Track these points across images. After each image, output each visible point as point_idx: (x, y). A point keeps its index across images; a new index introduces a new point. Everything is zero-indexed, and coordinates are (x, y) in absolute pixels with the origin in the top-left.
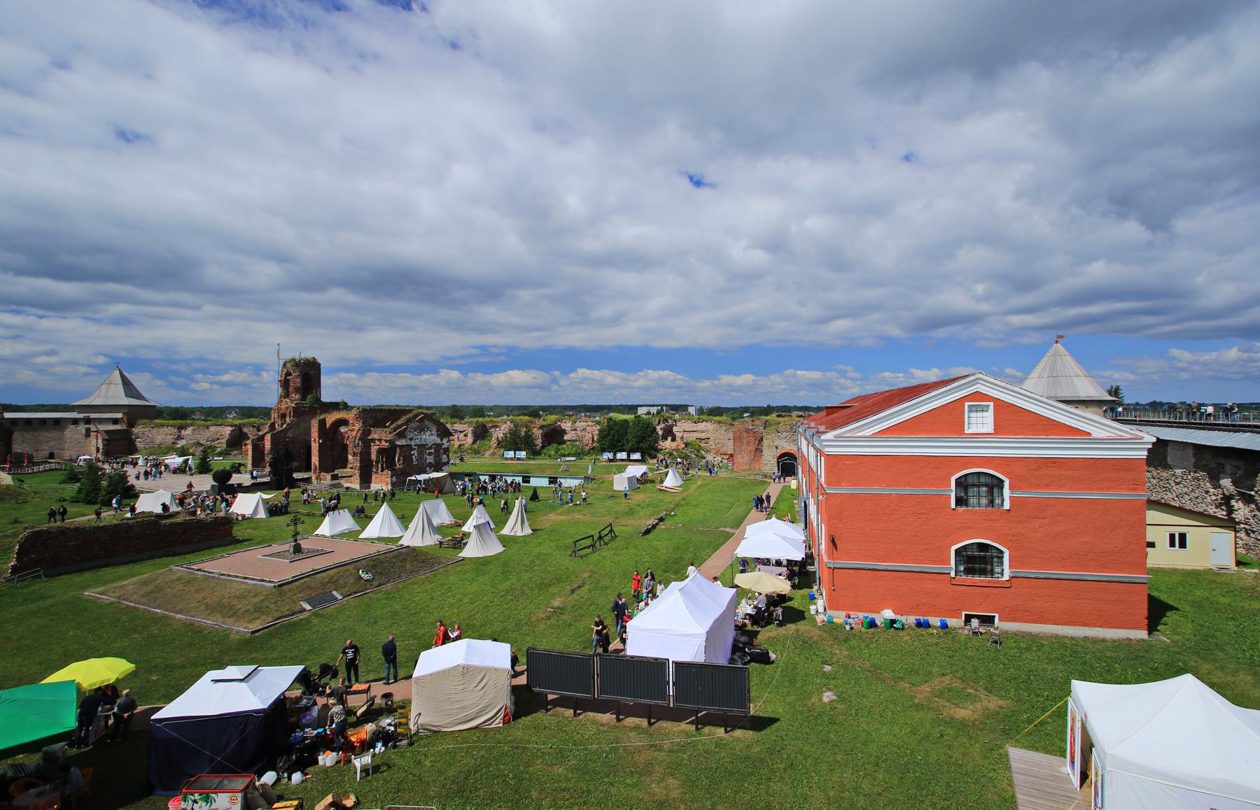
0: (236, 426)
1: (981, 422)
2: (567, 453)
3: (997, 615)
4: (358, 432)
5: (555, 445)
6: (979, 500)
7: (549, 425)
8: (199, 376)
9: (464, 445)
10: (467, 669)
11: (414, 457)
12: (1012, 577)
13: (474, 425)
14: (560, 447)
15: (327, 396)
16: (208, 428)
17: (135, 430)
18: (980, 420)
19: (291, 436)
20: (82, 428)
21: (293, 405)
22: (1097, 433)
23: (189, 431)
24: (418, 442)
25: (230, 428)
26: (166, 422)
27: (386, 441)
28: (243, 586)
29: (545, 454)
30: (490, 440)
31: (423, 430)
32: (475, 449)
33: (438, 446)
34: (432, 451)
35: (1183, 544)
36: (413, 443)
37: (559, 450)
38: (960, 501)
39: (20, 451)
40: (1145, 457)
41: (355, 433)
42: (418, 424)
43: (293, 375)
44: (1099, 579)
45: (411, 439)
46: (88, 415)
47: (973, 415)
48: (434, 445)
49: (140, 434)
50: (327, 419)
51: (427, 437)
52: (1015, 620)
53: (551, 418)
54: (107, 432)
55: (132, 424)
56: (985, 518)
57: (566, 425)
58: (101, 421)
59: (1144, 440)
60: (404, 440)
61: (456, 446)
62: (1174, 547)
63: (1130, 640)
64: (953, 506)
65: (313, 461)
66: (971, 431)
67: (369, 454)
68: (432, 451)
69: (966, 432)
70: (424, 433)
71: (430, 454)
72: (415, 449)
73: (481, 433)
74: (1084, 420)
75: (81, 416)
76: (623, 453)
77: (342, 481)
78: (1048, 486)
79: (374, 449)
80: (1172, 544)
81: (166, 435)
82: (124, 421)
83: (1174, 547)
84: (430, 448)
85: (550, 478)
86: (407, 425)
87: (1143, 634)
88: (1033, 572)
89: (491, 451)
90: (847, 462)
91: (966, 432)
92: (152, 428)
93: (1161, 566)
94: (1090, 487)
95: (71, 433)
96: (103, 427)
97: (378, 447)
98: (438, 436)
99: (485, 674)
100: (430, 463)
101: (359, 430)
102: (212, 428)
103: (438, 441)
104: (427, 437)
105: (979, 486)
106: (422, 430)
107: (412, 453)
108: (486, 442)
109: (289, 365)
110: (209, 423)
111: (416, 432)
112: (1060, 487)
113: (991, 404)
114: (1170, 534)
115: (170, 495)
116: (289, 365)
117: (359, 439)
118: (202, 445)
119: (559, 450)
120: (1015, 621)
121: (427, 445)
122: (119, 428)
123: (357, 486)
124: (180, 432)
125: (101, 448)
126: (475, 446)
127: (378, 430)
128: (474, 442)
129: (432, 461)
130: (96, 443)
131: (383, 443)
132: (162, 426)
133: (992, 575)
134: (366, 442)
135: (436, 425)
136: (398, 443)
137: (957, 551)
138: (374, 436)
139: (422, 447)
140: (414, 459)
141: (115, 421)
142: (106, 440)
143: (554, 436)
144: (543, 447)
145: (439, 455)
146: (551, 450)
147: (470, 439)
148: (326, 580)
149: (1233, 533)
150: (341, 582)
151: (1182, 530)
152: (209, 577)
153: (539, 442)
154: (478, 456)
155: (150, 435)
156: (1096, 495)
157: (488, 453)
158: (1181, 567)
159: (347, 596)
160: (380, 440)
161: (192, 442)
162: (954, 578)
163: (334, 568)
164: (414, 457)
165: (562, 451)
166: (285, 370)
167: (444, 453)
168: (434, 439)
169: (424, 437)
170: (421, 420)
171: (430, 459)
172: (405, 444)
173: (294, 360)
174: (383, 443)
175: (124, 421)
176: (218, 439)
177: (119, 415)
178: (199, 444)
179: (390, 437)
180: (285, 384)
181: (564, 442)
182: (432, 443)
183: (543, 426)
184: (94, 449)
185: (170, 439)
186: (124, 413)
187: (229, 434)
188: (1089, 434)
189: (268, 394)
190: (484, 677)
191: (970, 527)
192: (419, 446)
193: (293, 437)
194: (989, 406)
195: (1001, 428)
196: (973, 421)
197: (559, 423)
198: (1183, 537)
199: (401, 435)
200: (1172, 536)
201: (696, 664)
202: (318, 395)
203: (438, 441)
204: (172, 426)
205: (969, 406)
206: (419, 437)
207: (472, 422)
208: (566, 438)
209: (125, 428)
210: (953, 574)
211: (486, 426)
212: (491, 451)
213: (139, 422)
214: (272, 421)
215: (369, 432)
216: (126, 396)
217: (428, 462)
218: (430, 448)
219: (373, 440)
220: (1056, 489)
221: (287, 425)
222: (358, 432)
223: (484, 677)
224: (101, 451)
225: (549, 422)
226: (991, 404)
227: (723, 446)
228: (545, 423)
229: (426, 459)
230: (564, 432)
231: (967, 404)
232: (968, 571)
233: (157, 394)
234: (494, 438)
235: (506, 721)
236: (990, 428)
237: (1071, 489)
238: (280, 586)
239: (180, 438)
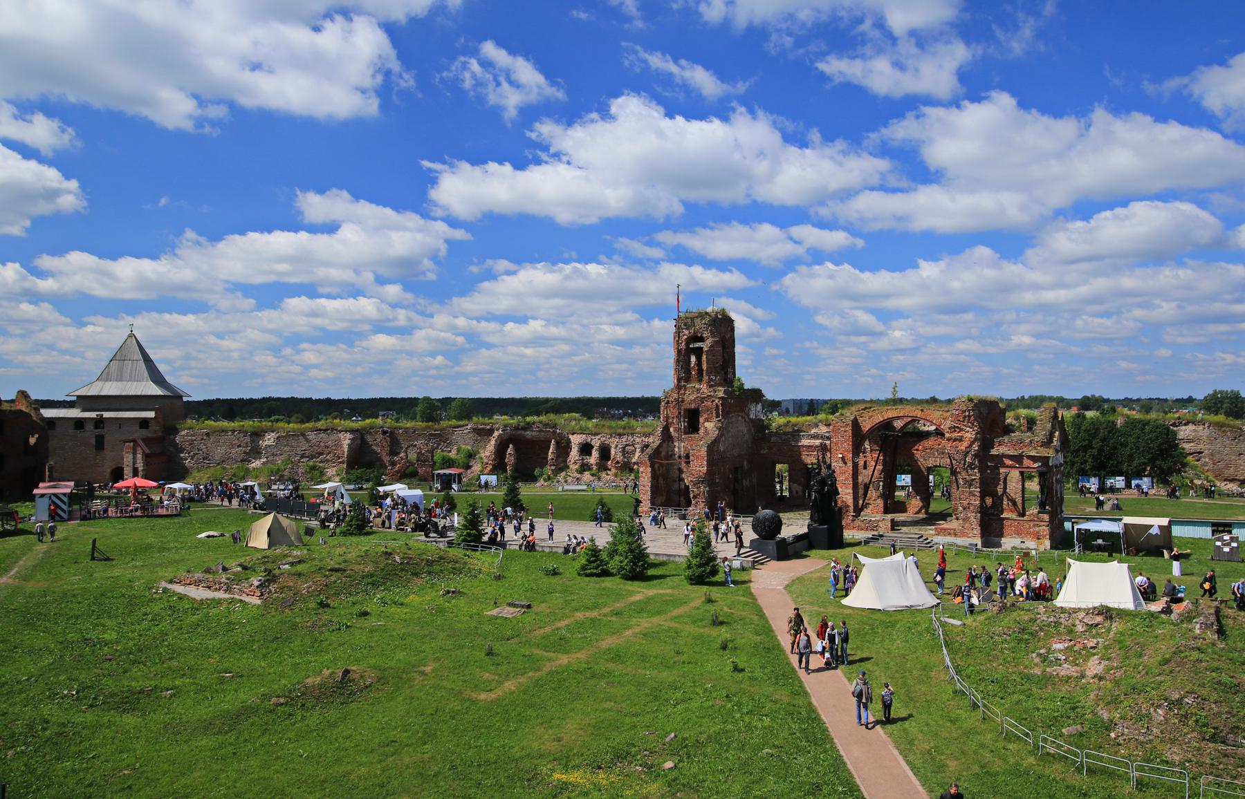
0: (357, 430)
4: (972, 443)
8: (305, 346)
21: (721, 394)
25: (349, 436)
27: (1033, 459)
41: (966, 444)
50: (860, 420)
75: (93, 415)
76: (1117, 478)
81: (232, 446)
85: (1214, 525)
101: (976, 439)
117: (976, 456)
125: (141, 469)
141: (144, 423)
155: (202, 446)
160: (1018, 459)
166: (686, 332)
173: (707, 313)
176: (321, 454)
177: (151, 414)
187: (349, 445)
193: (724, 451)
219: (1001, 457)
227: (1227, 467)
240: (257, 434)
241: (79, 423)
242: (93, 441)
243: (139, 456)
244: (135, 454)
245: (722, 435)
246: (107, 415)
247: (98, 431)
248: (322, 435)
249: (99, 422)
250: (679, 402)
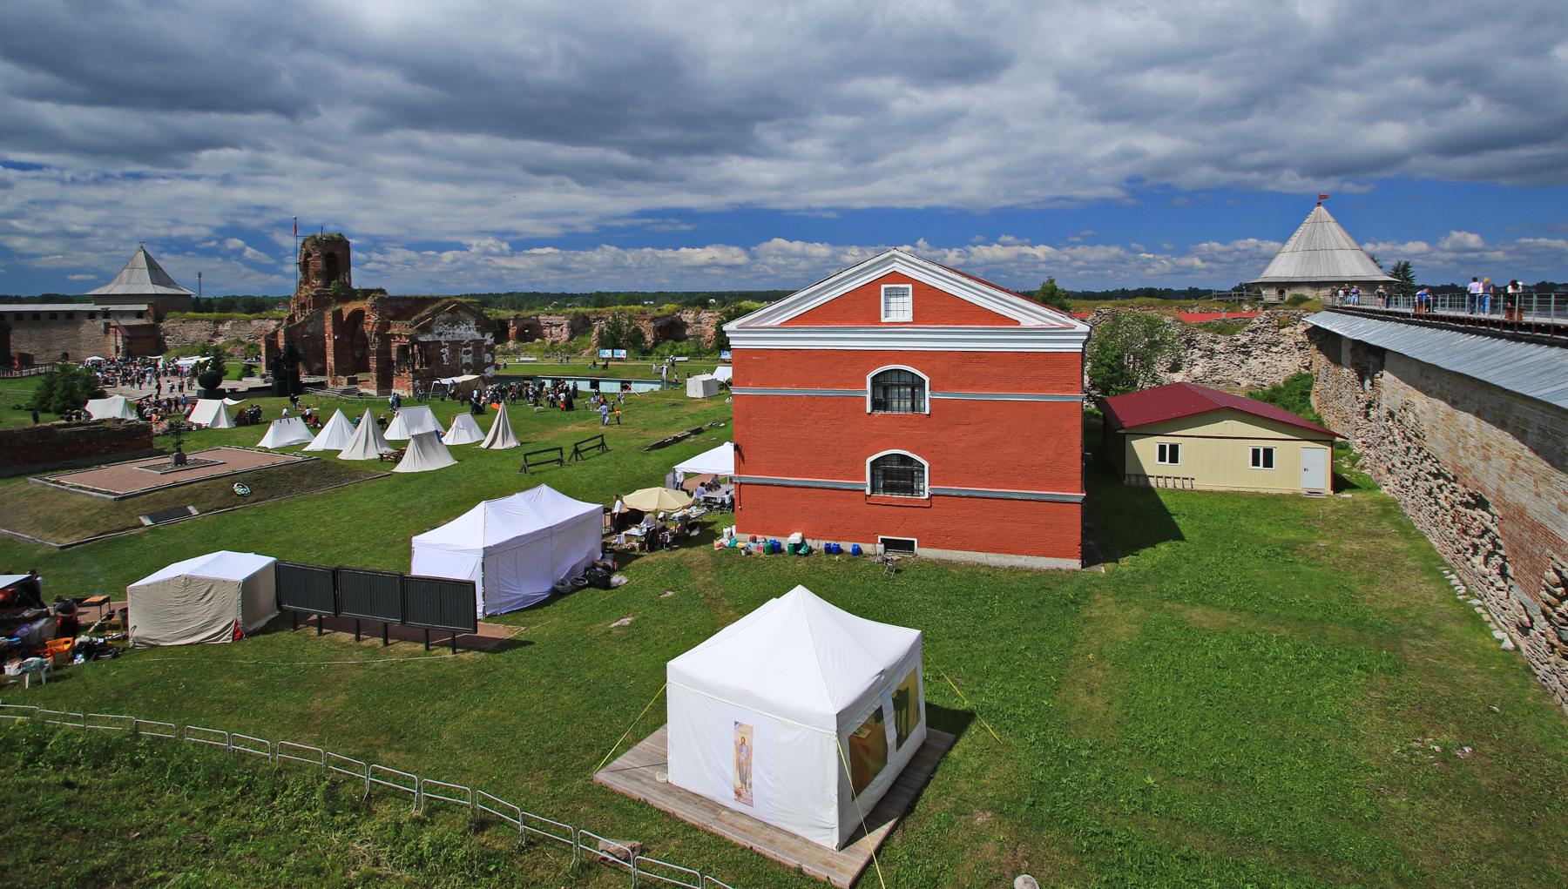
1: (900, 309)
2: (685, 352)
3: (915, 540)
4: (373, 326)
5: (671, 342)
6: (900, 405)
7: (665, 316)
9: (557, 341)
10: (190, 580)
11: (444, 356)
12: (932, 495)
13: (571, 316)
14: (678, 344)
15: (358, 280)
16: (249, 322)
17: (163, 325)
18: (900, 307)
19: (310, 331)
20: (100, 323)
22: (1027, 321)
23: (227, 326)
24: (450, 338)
26: (201, 314)
28: (86, 499)
29: (658, 353)
30: (590, 336)
31: (457, 323)
32: (571, 347)
33: (478, 344)
34: (470, 348)
35: (1268, 463)
36: (442, 339)
37: (675, 347)
38: (877, 405)
39: (27, 352)
40: (1081, 351)
41: (371, 327)
42: (450, 315)
43: (313, 255)
44: (1027, 498)
45: (440, 334)
46: (107, 309)
47: (893, 300)
48: (472, 341)
49: (170, 330)
51: (463, 332)
52: (935, 546)
53: (668, 308)
54: (127, 327)
55: (159, 318)
56: (904, 424)
57: (688, 317)
58: (123, 314)
59: (1076, 330)
60: (430, 336)
61: (548, 344)
62: (1259, 465)
63: (1060, 570)
64: (869, 410)
65: (328, 361)
66: (887, 320)
67: (389, 352)
68: (470, 348)
69: (882, 321)
70: (458, 327)
71: (467, 353)
72: (445, 347)
73: (580, 327)
74: (1008, 304)
77: (359, 387)
78: (972, 386)
79: (395, 346)
80: (1256, 462)
82: (149, 314)
83: (1259, 465)
84: (467, 345)
86: (434, 317)
87: (1075, 564)
88: (955, 489)
89: (590, 350)
90: (754, 358)
91: (882, 321)
92: (184, 322)
93: (1241, 490)
94: (1019, 387)
95: (89, 329)
96: (124, 322)
97: (397, 344)
98: (477, 330)
99: (212, 585)
100: (467, 363)
101: (375, 323)
102: (255, 323)
103: (478, 336)
104: (463, 332)
105: (899, 386)
106: (455, 323)
107: (442, 351)
108: (587, 338)
109: (308, 243)
110: (251, 316)
111: (446, 326)
112: (986, 388)
113: (910, 286)
114: (1160, 446)
115: (123, 402)
116: (308, 243)
117: (376, 335)
118: (243, 343)
119: (675, 347)
120: (936, 547)
121: (463, 341)
122: (144, 323)
123: (374, 392)
124: (217, 327)
125: (121, 347)
126: (572, 344)
127: (399, 323)
128: (571, 338)
129: (469, 361)
130: (117, 341)
131: (404, 338)
132: (196, 319)
133: (913, 493)
134: (386, 339)
135: (475, 317)
136: (422, 339)
137: (873, 464)
138: (394, 331)
139: (456, 345)
140: (445, 358)
141: (140, 314)
142: (127, 337)
143: (671, 330)
144: (656, 344)
145: (480, 354)
146: (666, 347)
147: (565, 336)
148: (185, 494)
149: (1329, 448)
150: (206, 496)
151: (1268, 444)
152: (66, 493)
153: (649, 337)
154: (574, 355)
155: (181, 331)
156: (1020, 396)
157: (586, 352)
158: (1265, 491)
159: (206, 512)
160: (400, 336)
161: (233, 339)
162: (870, 496)
163: (203, 480)
164: (444, 356)
165: (679, 350)
167: (486, 352)
168: (472, 335)
169: (458, 331)
170: (451, 311)
171: (467, 359)
172: (431, 340)
174: (404, 338)
175: (149, 314)
177: (144, 307)
178: (240, 342)
179: (410, 331)
180: (304, 266)
181: (686, 338)
182: (470, 339)
183: (657, 318)
184: (113, 348)
185: (205, 336)
186: (149, 304)
188: (1018, 323)
189: (286, 280)
190: (209, 590)
191: (885, 436)
192: (451, 343)
194: (908, 288)
195: (920, 316)
196: (892, 307)
197: (679, 314)
198: (1268, 453)
199: (426, 329)
200: (1256, 452)
201: (433, 580)
202: (347, 280)
203: (478, 336)
204: (207, 320)
205: (885, 289)
206: (451, 331)
207: (569, 313)
208: (688, 332)
209: (151, 322)
210: (868, 491)
211: (588, 319)
212: (590, 350)
213: (169, 315)
214: (292, 313)
215: (389, 326)
216: (153, 283)
217: (464, 362)
218: (467, 345)
219: (393, 336)
220: (982, 390)
221: (306, 318)
222: (373, 326)
223: (209, 590)
224: (121, 351)
225: (665, 313)
226: (910, 286)
228: (658, 314)
229: (461, 359)
230: (685, 325)
231: (883, 287)
232: (889, 488)
233: (186, 276)
234: (594, 333)
235: (237, 636)
236: (908, 317)
237: (999, 389)
238: (120, 499)
239: (217, 334)
240: (218, 322)
241: (92, 315)
242: (102, 327)
243: (119, 338)
244: (116, 336)
245: (310, 322)
246: (112, 308)
247: (105, 320)
248: (263, 322)
249: (107, 314)
250: (298, 298)
